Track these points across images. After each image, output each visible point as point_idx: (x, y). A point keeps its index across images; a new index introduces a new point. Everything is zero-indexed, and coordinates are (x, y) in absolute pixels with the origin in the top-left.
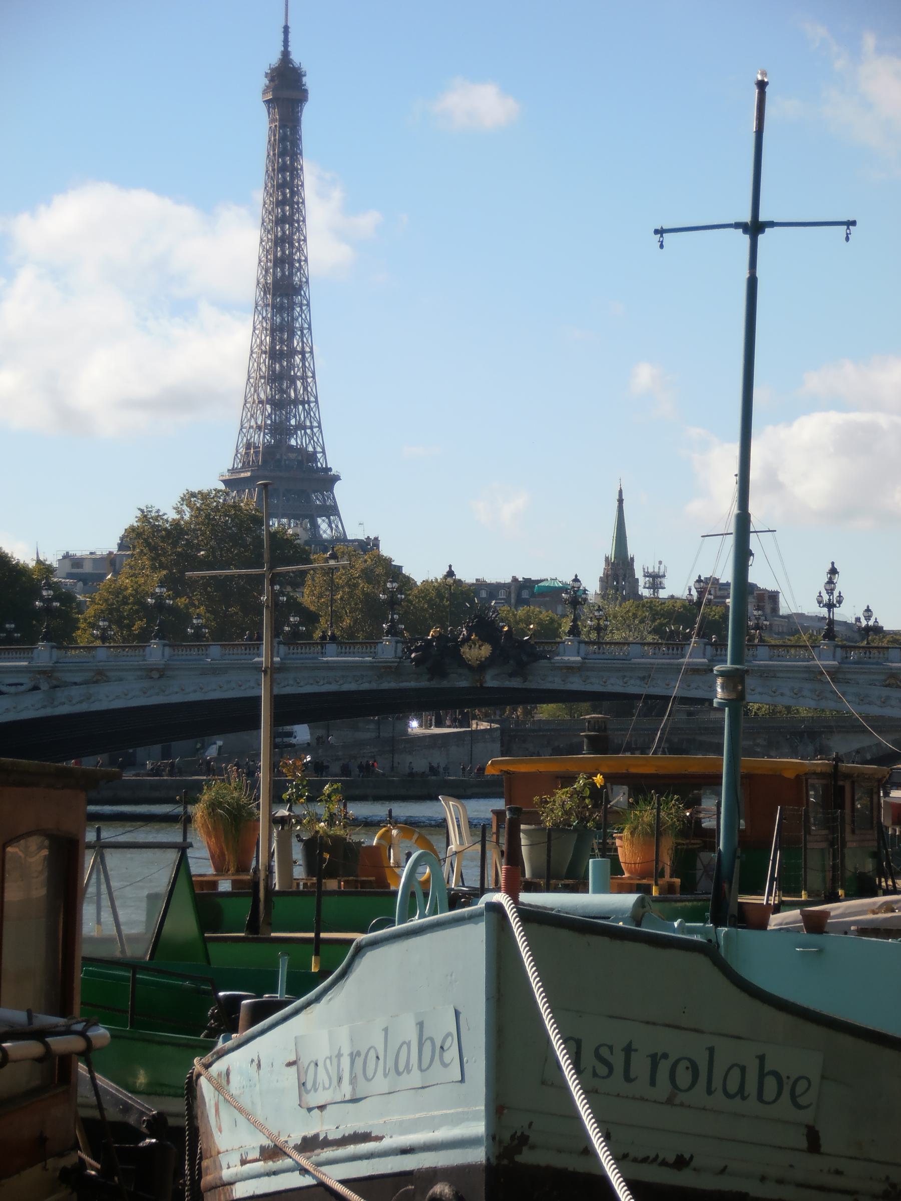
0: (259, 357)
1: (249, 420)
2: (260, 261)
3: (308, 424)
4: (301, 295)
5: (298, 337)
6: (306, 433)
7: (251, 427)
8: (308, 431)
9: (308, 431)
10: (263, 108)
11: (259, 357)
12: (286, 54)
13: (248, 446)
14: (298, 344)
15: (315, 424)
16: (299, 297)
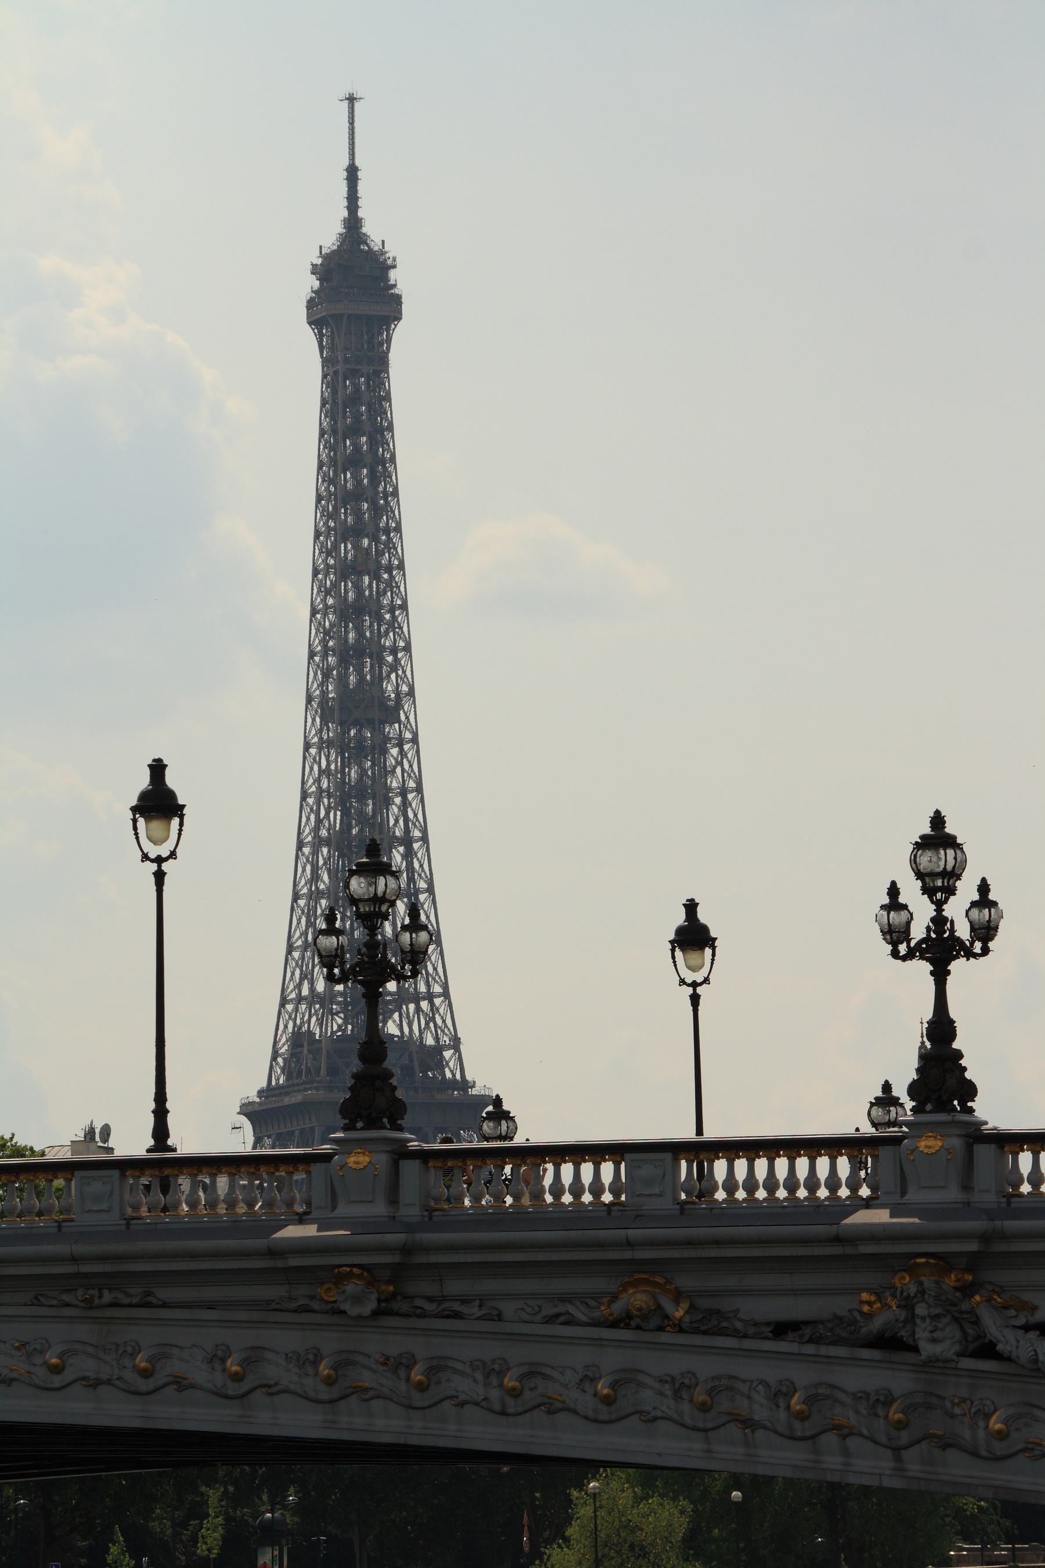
0: (315, 852)
1: (299, 986)
2: (312, 654)
3: (423, 988)
4: (399, 722)
5: (396, 810)
6: (418, 1009)
7: (300, 999)
8: (424, 1005)
9: (424, 1005)
10: (309, 338)
11: (315, 852)
12: (353, 223)
13: (300, 1039)
14: (397, 821)
15: (437, 989)
16: (396, 725)
